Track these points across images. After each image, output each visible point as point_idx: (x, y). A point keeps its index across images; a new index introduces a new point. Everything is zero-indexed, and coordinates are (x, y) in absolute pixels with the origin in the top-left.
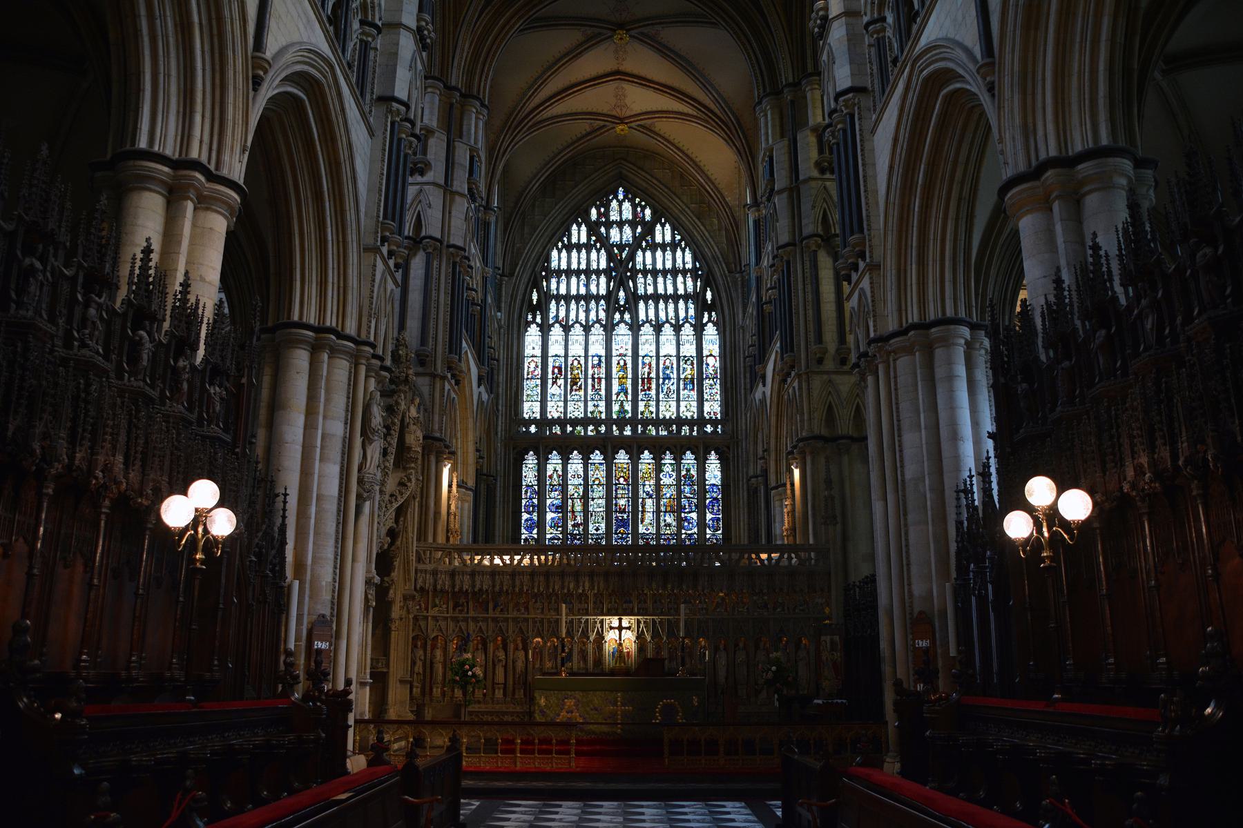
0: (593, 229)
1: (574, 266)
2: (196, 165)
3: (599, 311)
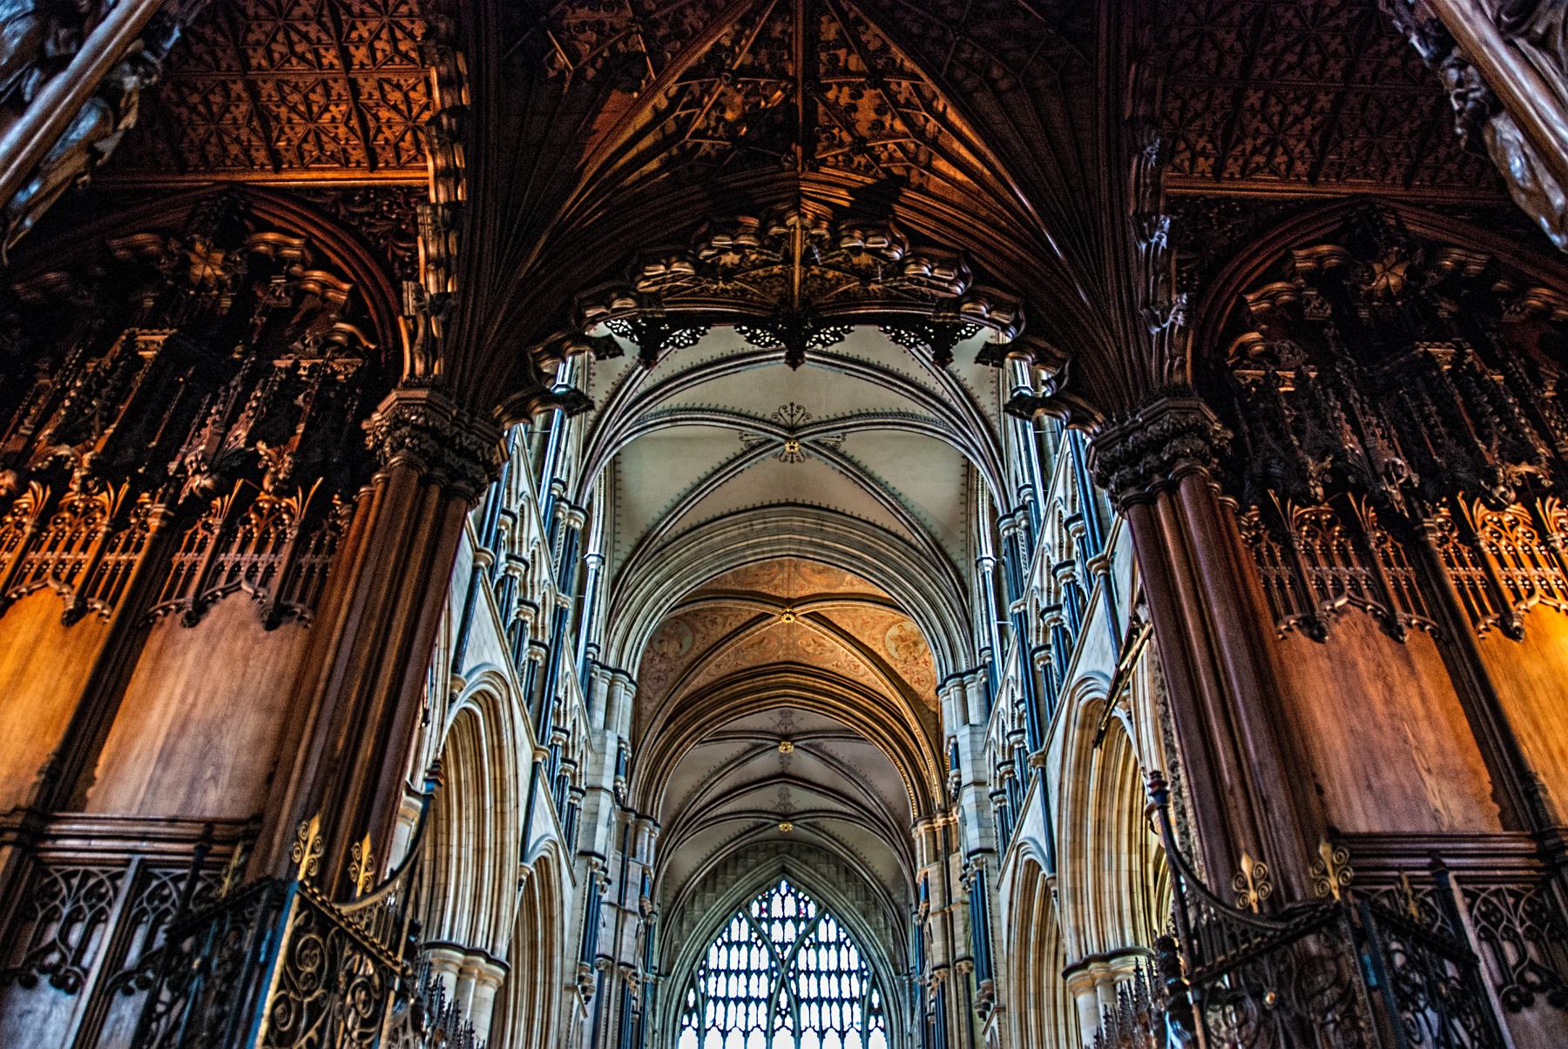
0: (754, 924)
1: (734, 966)
2: (479, 952)
3: (759, 1014)
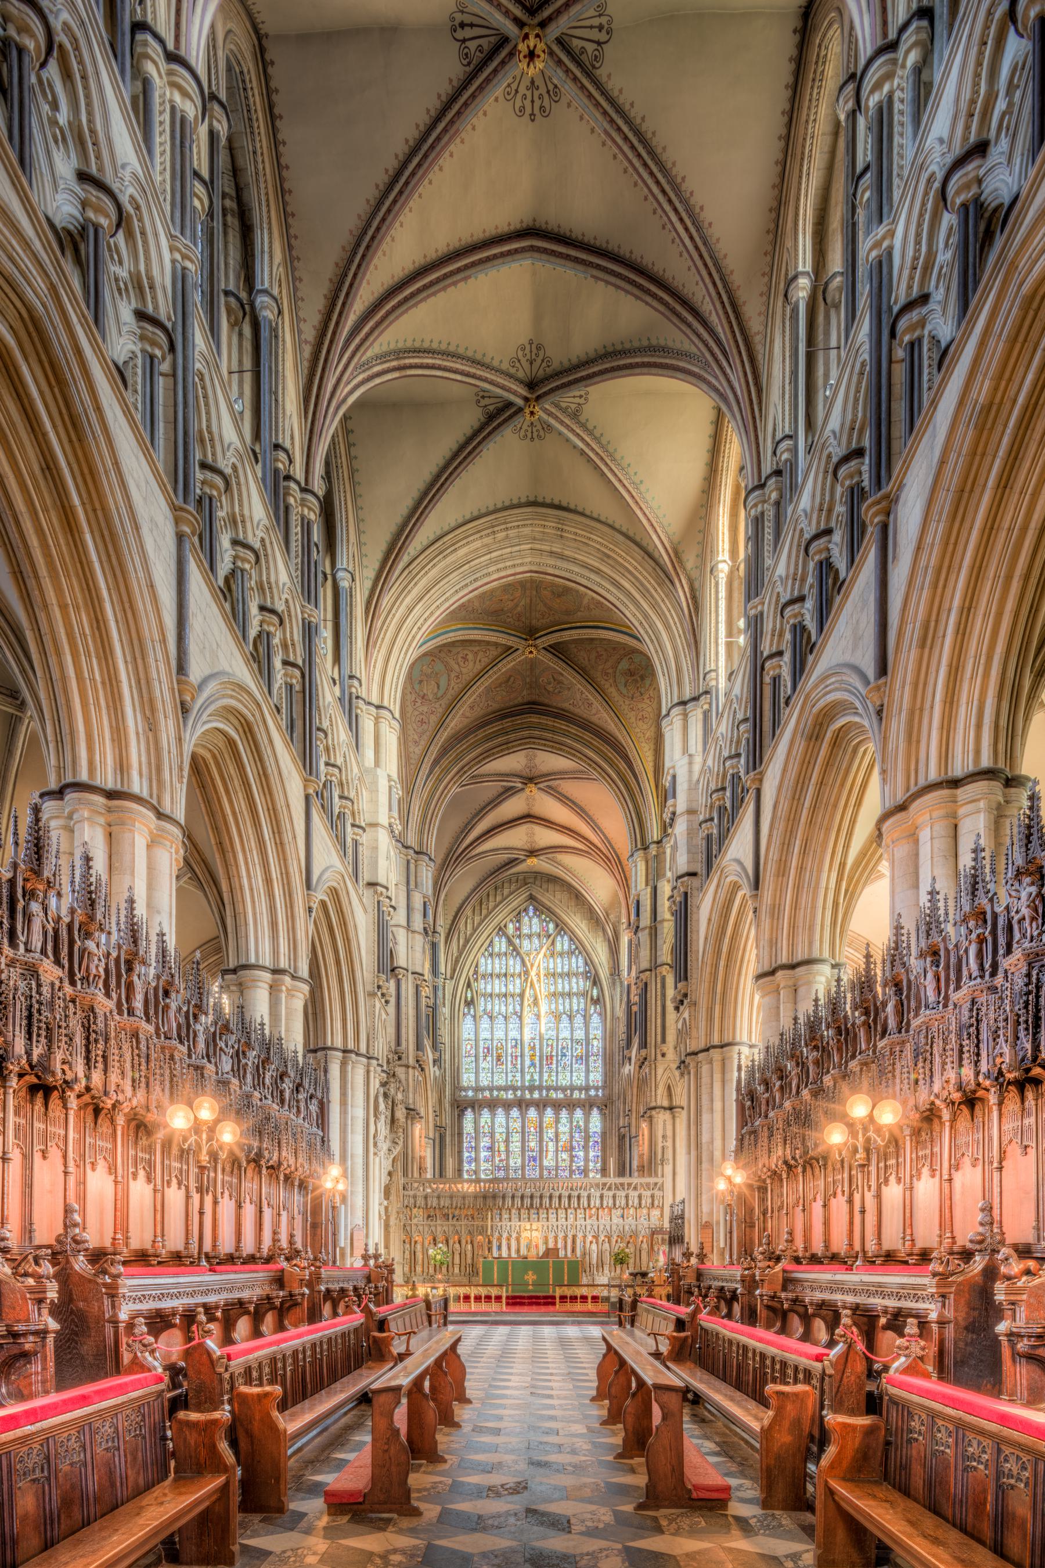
0: (510, 942)
1: (497, 971)
